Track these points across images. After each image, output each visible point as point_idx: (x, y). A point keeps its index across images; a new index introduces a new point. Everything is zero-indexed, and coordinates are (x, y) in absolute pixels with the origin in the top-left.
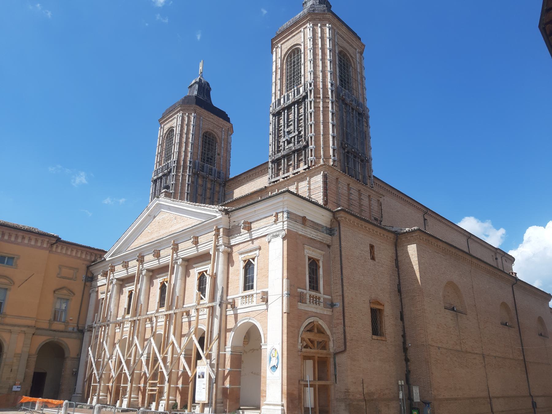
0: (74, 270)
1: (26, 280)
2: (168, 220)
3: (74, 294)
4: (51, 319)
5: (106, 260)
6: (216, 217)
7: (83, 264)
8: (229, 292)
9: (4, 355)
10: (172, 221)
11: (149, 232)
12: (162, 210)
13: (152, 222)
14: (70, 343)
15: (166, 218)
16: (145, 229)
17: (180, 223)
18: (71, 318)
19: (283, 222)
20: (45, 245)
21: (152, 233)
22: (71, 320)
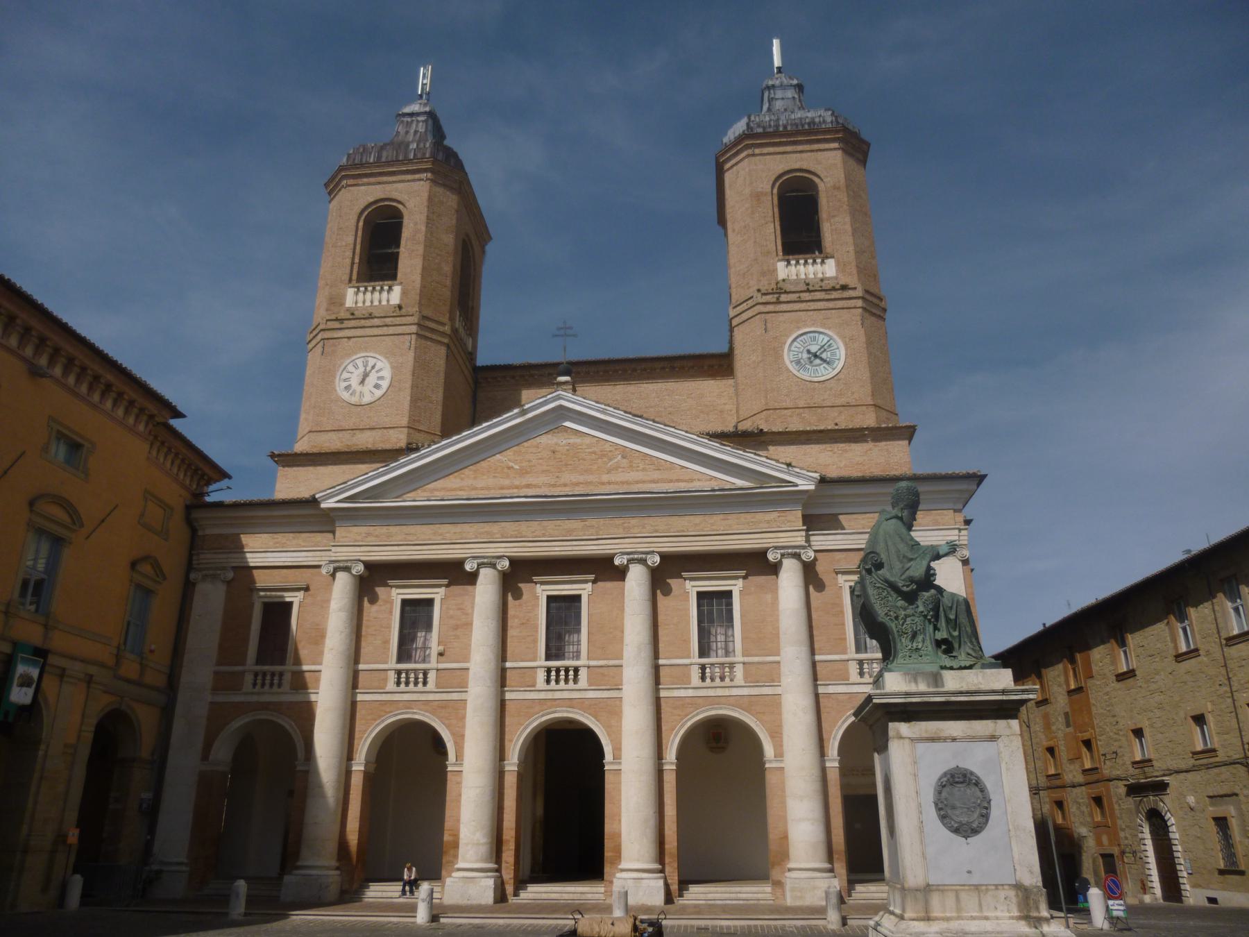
0: (165, 510)
1: (103, 521)
2: (594, 453)
3: (165, 578)
4: (119, 644)
5: (323, 505)
6: (797, 486)
7: (180, 496)
8: (816, 646)
9: (43, 747)
10: (610, 460)
11: (509, 468)
12: (568, 424)
13: (525, 444)
14: (146, 718)
15: (586, 447)
16: (494, 455)
17: (644, 470)
18: (153, 647)
19: (960, 530)
20: (141, 427)
21: (523, 472)
22: (152, 651)
